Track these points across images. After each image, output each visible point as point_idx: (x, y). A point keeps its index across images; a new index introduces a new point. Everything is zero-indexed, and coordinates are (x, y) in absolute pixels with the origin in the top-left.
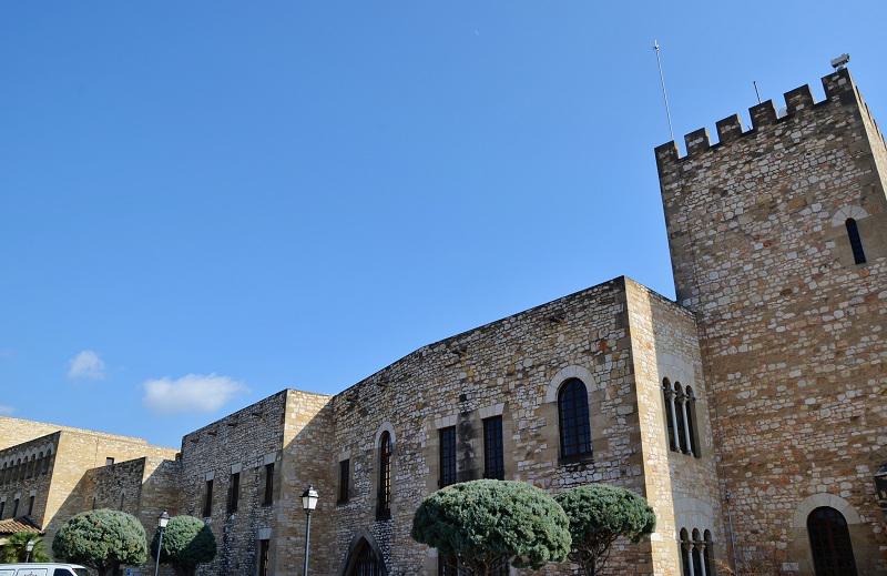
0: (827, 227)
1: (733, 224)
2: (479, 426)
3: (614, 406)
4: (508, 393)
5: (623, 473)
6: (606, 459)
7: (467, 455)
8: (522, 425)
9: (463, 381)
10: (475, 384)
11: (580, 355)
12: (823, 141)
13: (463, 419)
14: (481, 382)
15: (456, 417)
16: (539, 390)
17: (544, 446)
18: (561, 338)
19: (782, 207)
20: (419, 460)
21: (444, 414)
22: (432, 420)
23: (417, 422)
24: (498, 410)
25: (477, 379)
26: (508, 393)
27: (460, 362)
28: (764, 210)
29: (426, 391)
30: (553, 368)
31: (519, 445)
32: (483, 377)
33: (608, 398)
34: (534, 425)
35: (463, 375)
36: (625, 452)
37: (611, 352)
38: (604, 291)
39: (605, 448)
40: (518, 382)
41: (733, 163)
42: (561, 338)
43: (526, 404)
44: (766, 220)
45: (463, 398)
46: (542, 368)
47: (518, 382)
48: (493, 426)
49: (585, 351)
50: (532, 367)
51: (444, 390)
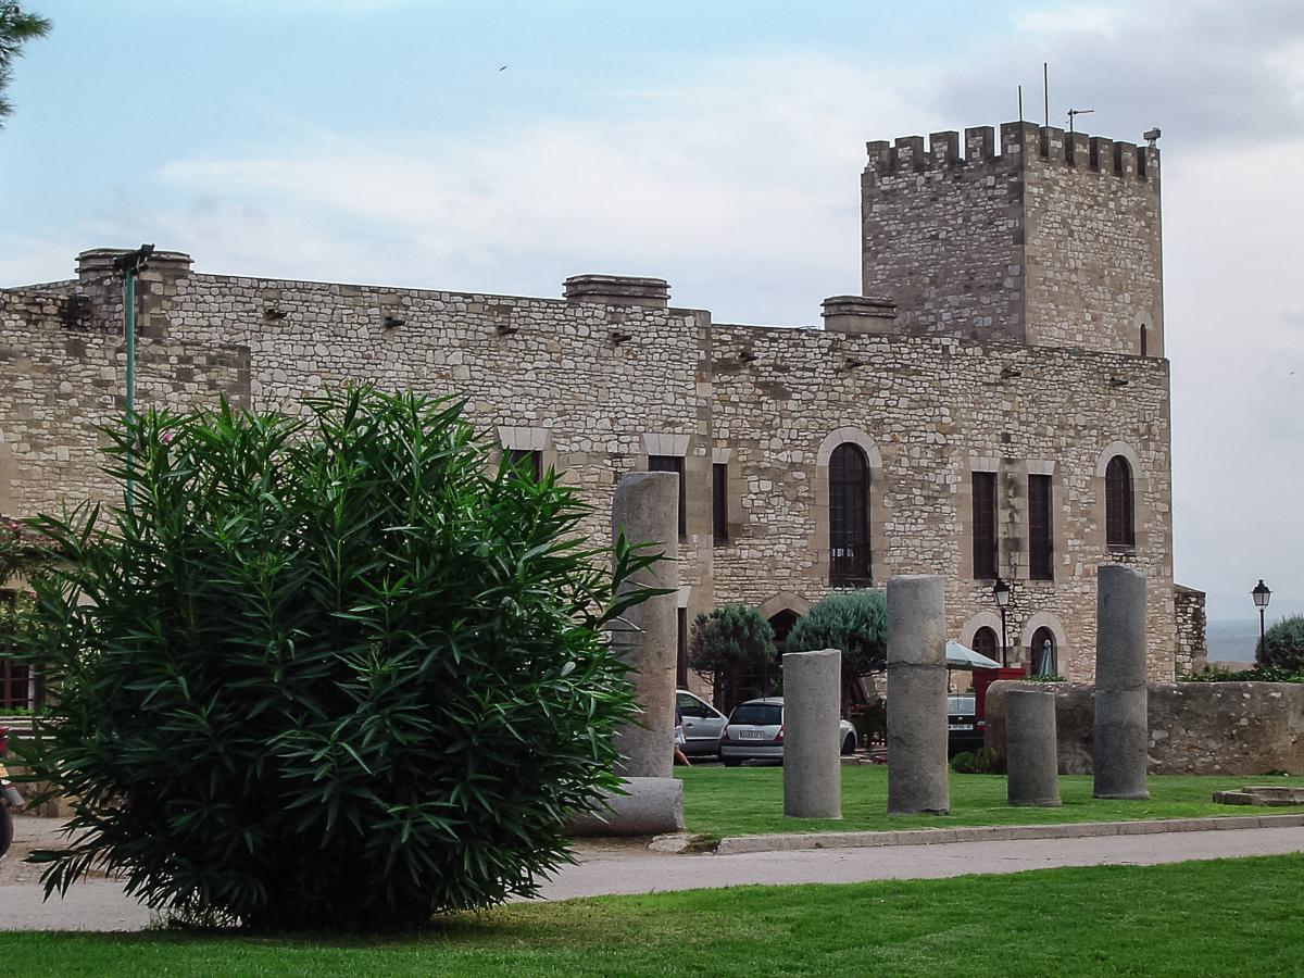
0: (1131, 323)
1: (1074, 278)
2: (1025, 483)
3: (1155, 500)
4: (1059, 450)
5: (1159, 573)
6: (1146, 555)
7: (1011, 516)
8: (1073, 495)
9: (1006, 413)
10: (1021, 423)
11: (1129, 432)
12: (1138, 224)
13: (1007, 468)
14: (1027, 423)
15: (997, 462)
16: (1091, 459)
17: (1093, 527)
18: (1113, 403)
19: (1107, 280)
20: (946, 509)
21: (982, 451)
22: (965, 456)
23: (942, 452)
24: (1048, 469)
25: (1023, 418)
26: (1059, 450)
27: (1002, 384)
28: (1096, 275)
29: (957, 409)
30: (1104, 437)
31: (1069, 519)
32: (1031, 418)
33: (1150, 490)
34: (1084, 499)
35: (1007, 406)
36: (1160, 551)
37: (1153, 440)
38: (1152, 368)
39: (1145, 543)
40: (1069, 440)
41: (1081, 199)
42: (1113, 403)
43: (1078, 471)
44: (1096, 290)
45: (1006, 438)
46: (1094, 432)
47: (1069, 440)
48: (1041, 487)
49: (1133, 430)
50: (1085, 427)
51: (980, 417)
